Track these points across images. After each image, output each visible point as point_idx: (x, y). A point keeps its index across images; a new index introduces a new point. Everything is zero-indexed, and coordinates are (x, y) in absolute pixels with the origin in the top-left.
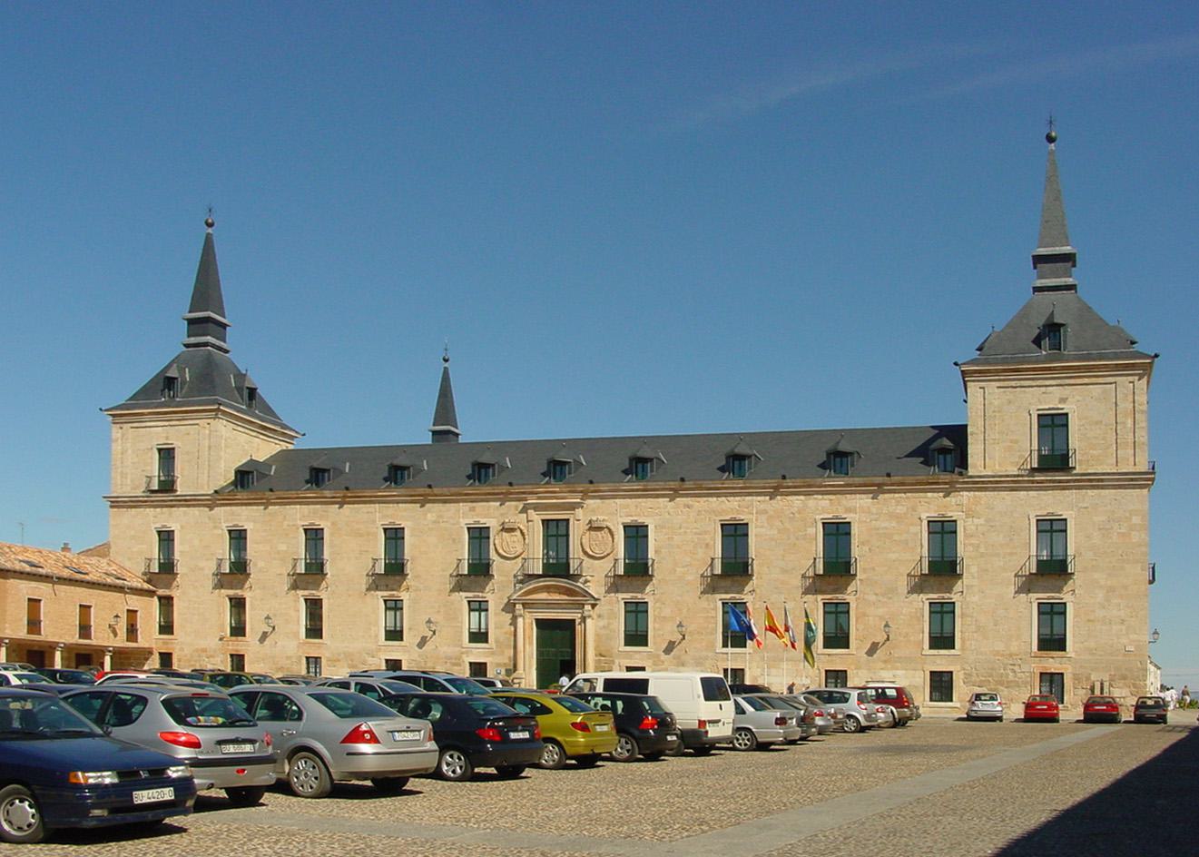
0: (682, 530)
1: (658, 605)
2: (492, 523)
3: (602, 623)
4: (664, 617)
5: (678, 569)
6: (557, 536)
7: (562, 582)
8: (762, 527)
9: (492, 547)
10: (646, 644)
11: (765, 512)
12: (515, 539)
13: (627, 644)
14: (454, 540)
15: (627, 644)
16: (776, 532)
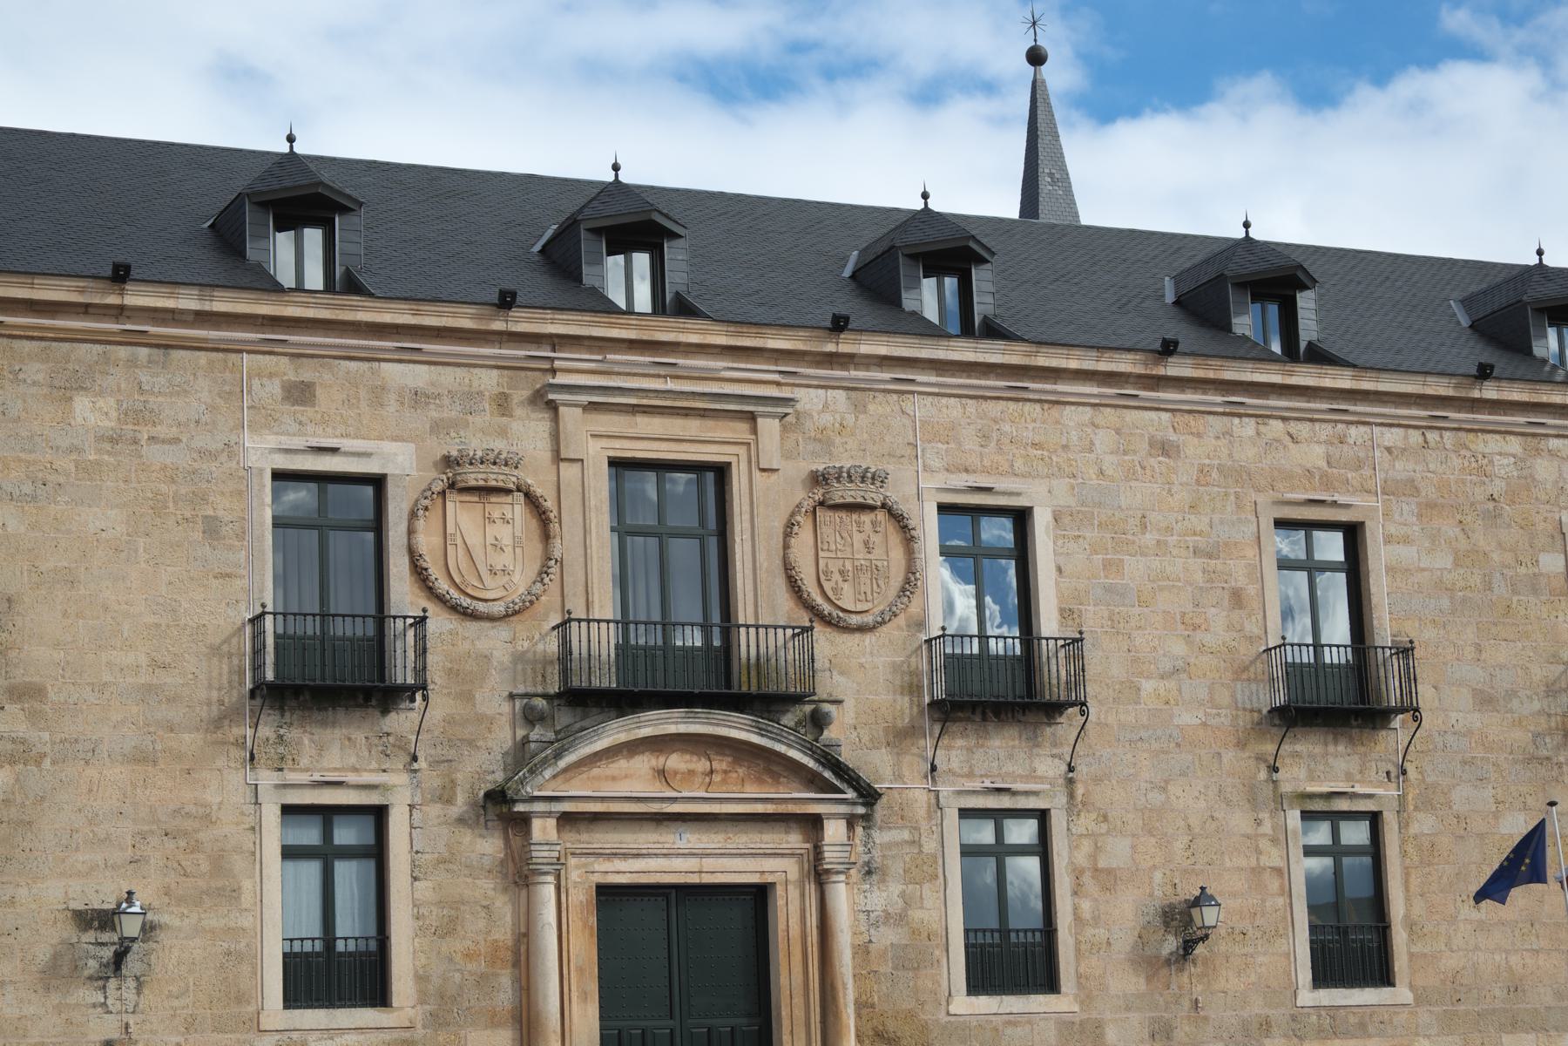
0: (1150, 538)
1: (1086, 822)
2: (402, 461)
3: (880, 898)
4: (1109, 871)
5: (1148, 686)
6: (661, 534)
7: (736, 727)
8: (1406, 540)
9: (398, 566)
10: (1049, 983)
11: (1411, 487)
12: (504, 533)
13: (977, 985)
14: (212, 529)
15: (977, 985)
16: (1448, 562)
